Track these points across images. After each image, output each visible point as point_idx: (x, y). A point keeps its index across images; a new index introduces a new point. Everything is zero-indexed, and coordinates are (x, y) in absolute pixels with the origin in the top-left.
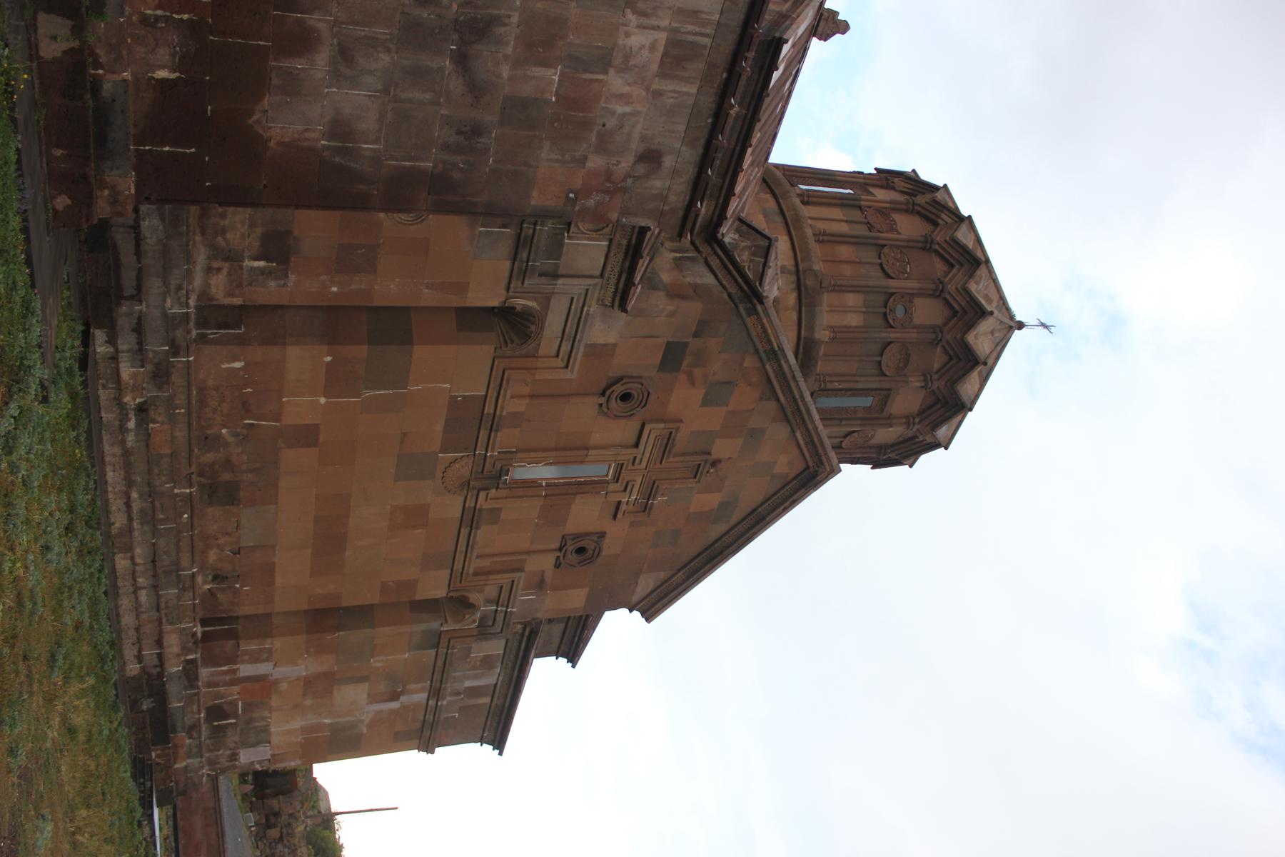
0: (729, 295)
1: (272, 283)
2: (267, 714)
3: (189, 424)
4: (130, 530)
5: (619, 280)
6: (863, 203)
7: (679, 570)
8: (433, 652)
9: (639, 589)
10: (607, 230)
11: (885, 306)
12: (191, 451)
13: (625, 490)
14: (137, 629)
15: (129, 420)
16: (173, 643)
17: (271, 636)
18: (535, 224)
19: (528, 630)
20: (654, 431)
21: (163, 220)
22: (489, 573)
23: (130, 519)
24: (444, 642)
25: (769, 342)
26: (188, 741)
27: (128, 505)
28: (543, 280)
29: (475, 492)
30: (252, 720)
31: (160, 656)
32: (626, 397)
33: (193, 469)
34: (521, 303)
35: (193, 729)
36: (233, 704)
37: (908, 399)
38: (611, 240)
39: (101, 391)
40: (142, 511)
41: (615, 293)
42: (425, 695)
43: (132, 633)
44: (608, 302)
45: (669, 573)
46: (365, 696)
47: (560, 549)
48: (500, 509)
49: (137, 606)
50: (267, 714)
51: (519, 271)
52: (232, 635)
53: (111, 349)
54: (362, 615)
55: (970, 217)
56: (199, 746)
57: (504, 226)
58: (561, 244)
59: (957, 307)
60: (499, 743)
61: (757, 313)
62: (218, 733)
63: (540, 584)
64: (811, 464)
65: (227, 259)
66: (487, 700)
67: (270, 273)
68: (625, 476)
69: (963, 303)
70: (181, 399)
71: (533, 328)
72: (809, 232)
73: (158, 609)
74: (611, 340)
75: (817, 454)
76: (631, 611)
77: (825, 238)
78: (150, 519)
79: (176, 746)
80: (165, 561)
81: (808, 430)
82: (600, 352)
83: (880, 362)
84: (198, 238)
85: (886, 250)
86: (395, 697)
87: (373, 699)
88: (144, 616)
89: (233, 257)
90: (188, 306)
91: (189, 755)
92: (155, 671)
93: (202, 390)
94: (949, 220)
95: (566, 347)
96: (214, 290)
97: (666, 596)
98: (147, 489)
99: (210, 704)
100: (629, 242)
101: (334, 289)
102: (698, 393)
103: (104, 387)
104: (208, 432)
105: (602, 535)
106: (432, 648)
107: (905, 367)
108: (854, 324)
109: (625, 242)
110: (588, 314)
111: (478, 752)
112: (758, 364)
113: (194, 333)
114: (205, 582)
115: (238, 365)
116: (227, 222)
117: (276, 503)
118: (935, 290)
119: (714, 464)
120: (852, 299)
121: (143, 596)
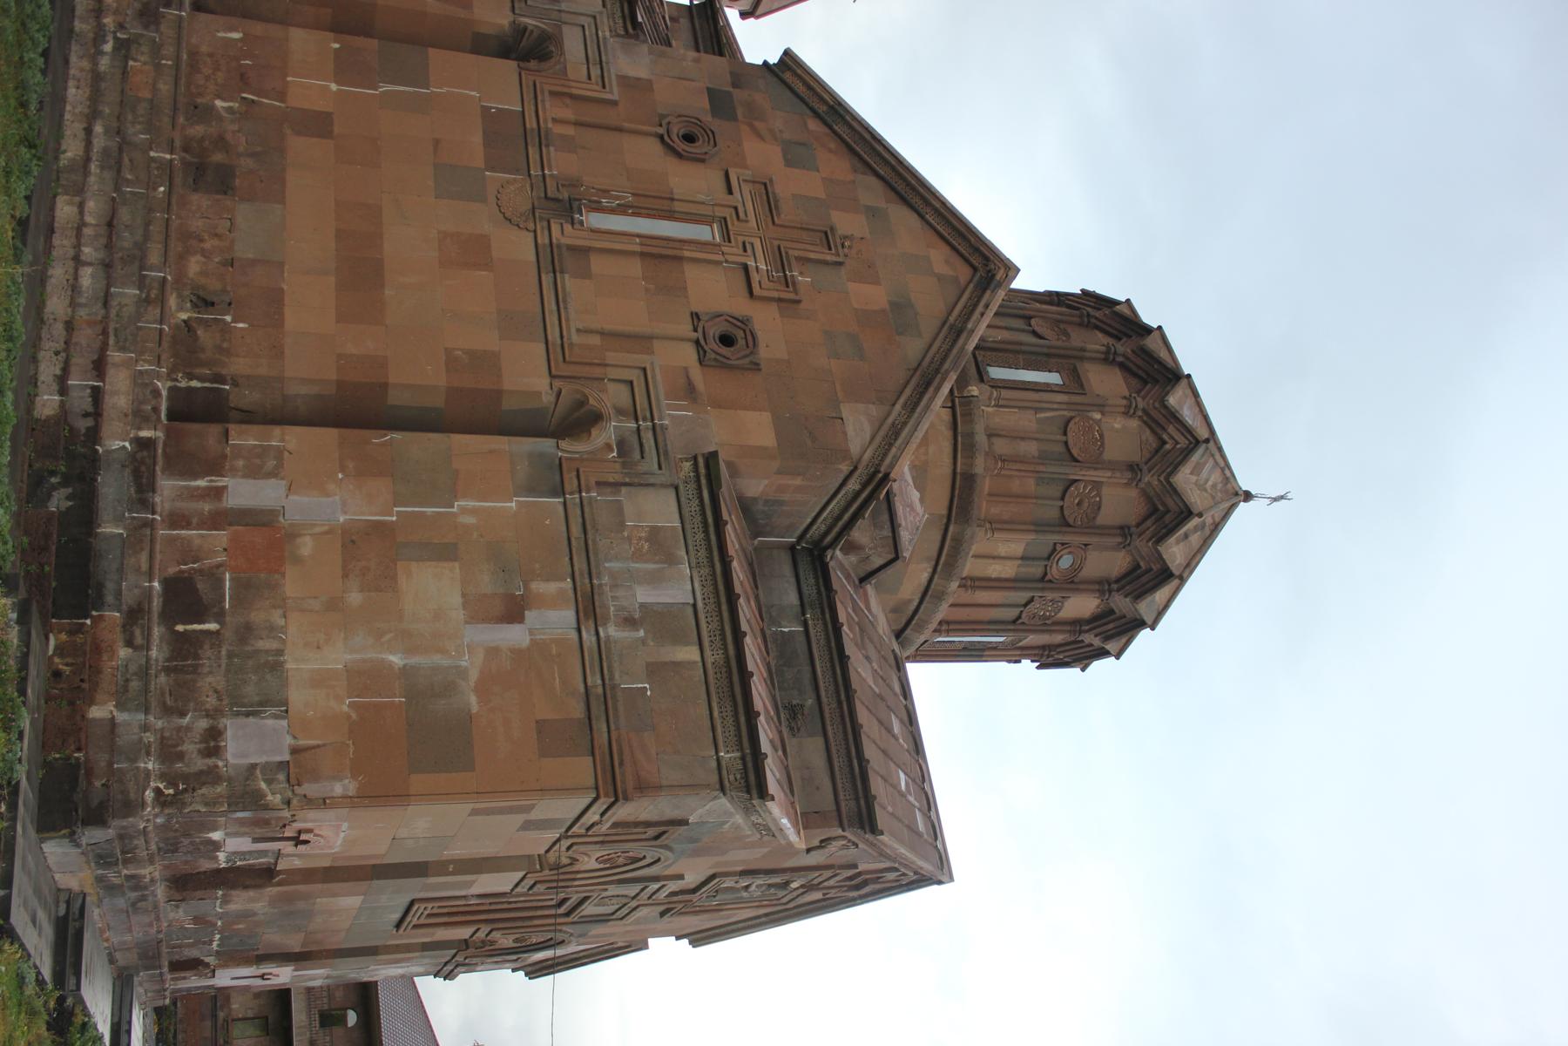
14: (69, 326)
24: (571, 483)
25: (822, 99)
26: (123, 652)
31: (97, 394)
42: (568, 616)
43: (59, 330)
49: (75, 288)
50: (277, 618)
62: (185, 649)
73: (106, 304)
75: (977, 250)
78: (113, 163)
80: (126, 240)
81: (936, 210)
88: (82, 313)
92: (83, 425)
95: (595, 72)
99: (172, 570)
102: (774, 153)
104: (199, 100)
106: (554, 494)
114: (181, 309)
115: (236, 35)
117: (282, 201)
121: (87, 278)
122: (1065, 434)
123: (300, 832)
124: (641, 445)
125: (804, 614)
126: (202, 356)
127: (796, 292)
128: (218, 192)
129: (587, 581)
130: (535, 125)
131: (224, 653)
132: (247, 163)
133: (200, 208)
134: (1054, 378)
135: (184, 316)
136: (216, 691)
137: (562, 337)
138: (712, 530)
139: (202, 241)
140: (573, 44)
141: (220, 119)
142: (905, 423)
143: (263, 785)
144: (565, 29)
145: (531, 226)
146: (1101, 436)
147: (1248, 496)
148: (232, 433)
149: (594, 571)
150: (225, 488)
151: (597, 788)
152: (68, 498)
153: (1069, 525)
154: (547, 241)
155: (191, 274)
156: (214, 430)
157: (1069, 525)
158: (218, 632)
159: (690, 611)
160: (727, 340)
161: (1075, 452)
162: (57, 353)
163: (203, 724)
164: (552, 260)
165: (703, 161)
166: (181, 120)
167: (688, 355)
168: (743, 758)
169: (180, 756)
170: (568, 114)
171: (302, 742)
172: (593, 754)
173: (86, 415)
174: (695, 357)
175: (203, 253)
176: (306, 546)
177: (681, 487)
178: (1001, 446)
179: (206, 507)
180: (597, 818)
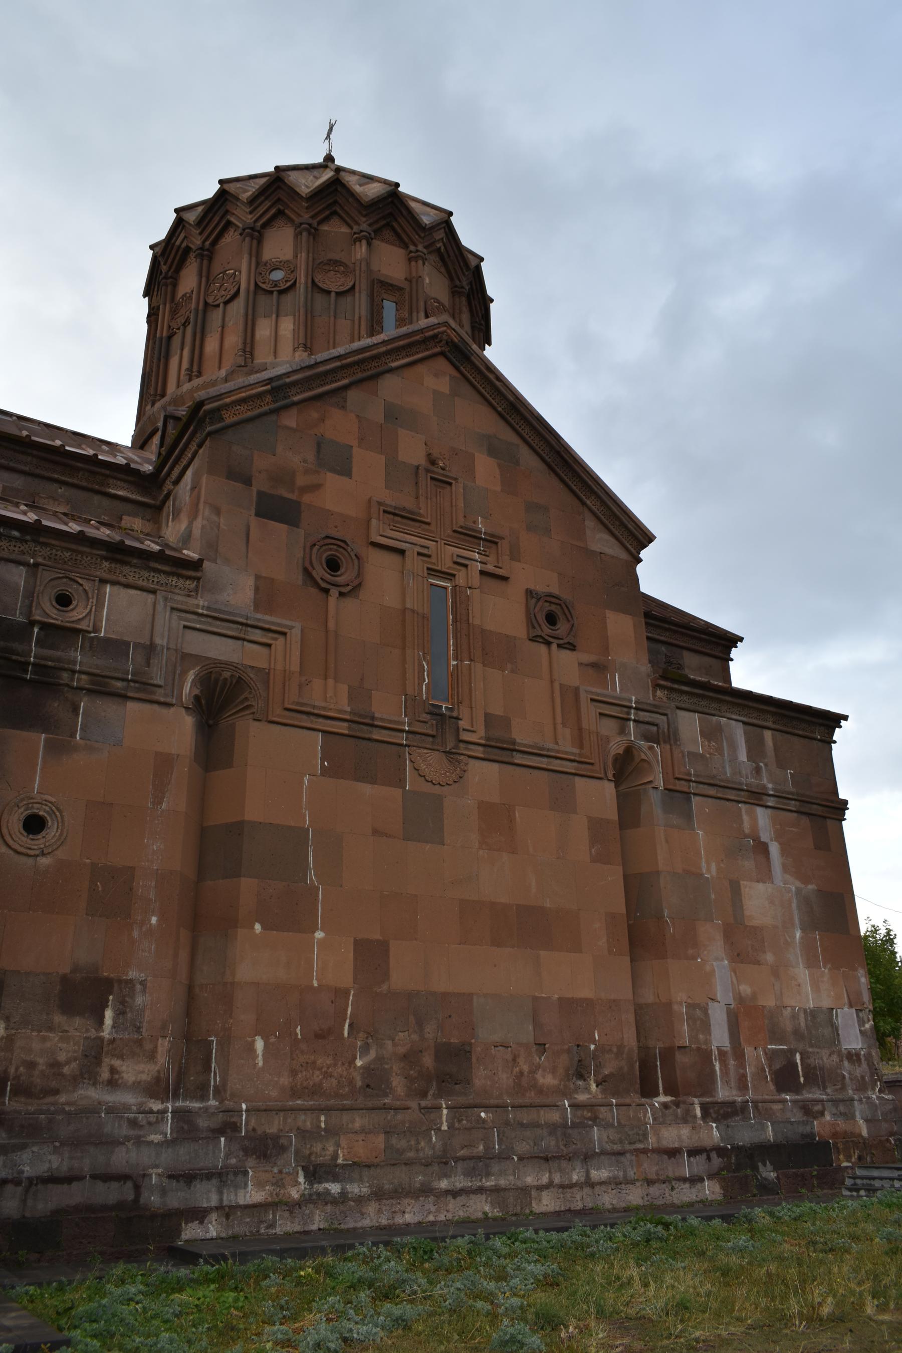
0: (200, 446)
1: (139, 1000)
2: (787, 1012)
3: (344, 1109)
4: (496, 1190)
5: (159, 571)
6: (165, 334)
7: (584, 504)
8: (695, 800)
9: (609, 551)
10: (87, 585)
11: (267, 293)
12: (385, 1108)
13: (466, 566)
14: (650, 1182)
15: (327, 1192)
16: (675, 1135)
17: (669, 1004)
18: (74, 672)
19: (662, 682)
20: (380, 531)
21: (24, 1147)
22: (580, 729)
23: (481, 1190)
24: (682, 786)
25: (260, 396)
26: (828, 1117)
27: (455, 1193)
28: (154, 661)
29: (462, 745)
30: (796, 1032)
31: (694, 1152)
32: (333, 565)
33: (413, 1104)
34: (188, 688)
35: (808, 1110)
36: (771, 1056)
37: (390, 261)
38: (103, 581)
39: (278, 1230)
40: (469, 1174)
41: (179, 576)
42: (760, 811)
43: (654, 1190)
44: (191, 585)
45: (587, 514)
46: (761, 886)
47: (548, 644)
48: (487, 715)
49: (615, 1183)
50: (787, 1012)
51: (143, 689)
52: (668, 1054)
53: (214, 1216)
54: (638, 889)
55: (177, 211)
56: (835, 1102)
57: (75, 710)
58: (107, 641)
59: (273, 211)
60: (831, 721)
61: (218, 409)
62: (815, 1077)
63: (599, 668)
64: (438, 350)
65: (98, 1061)
66: (768, 734)
67: (123, 1002)
68: (446, 565)
69: (268, 204)
70: (305, 1121)
71: (226, 674)
72: (187, 387)
74: (251, 582)
75: (425, 341)
76: (640, 560)
77: (195, 368)
78: (479, 1164)
79: (835, 1135)
80: (549, 1143)
81: (388, 353)
82: (267, 594)
83: (338, 294)
84: (62, 1098)
85: (210, 300)
86: (762, 849)
87: (765, 875)
88: (631, 1174)
89: (95, 1053)
90: (165, 1111)
91: (849, 1116)
92: (717, 1161)
93: (295, 1092)
94: (182, 235)
95: (257, 635)
96: (144, 1077)
97: (618, 518)
98: (436, 1168)
99: (772, 1087)
100: (106, 559)
101: (154, 920)
102: (332, 480)
103: (272, 1226)
104: (359, 1083)
105: (529, 593)
106: (689, 800)
107: (346, 266)
108: (291, 327)
109: (106, 564)
110: (208, 608)
111: (845, 748)
112: (294, 411)
113: (213, 1103)
114: (587, 1089)
115: (259, 1044)
116: (41, 1061)
117: (471, 995)
118: (252, 238)
119: (433, 462)
120: (264, 330)
124: (648, 723)
126: (626, 1069)
127: (502, 538)
128: (469, 1059)
129: (742, 793)
130: (346, 724)
131: (811, 1050)
132: (430, 1031)
133: (489, 1077)
135: (593, 1086)
136: (830, 1055)
137: (574, 761)
139: (521, 1073)
141: (380, 1059)
148: (681, 1043)
150: (718, 1048)
152: (765, 1165)
154: (481, 748)
155: (556, 1082)
156: (681, 1059)
158: (801, 1054)
162: (673, 1189)
163: (846, 1063)
169: (863, 1077)
173: (709, 1158)
174: (568, 652)
175: (533, 1072)
176: (745, 989)
179: (732, 1062)
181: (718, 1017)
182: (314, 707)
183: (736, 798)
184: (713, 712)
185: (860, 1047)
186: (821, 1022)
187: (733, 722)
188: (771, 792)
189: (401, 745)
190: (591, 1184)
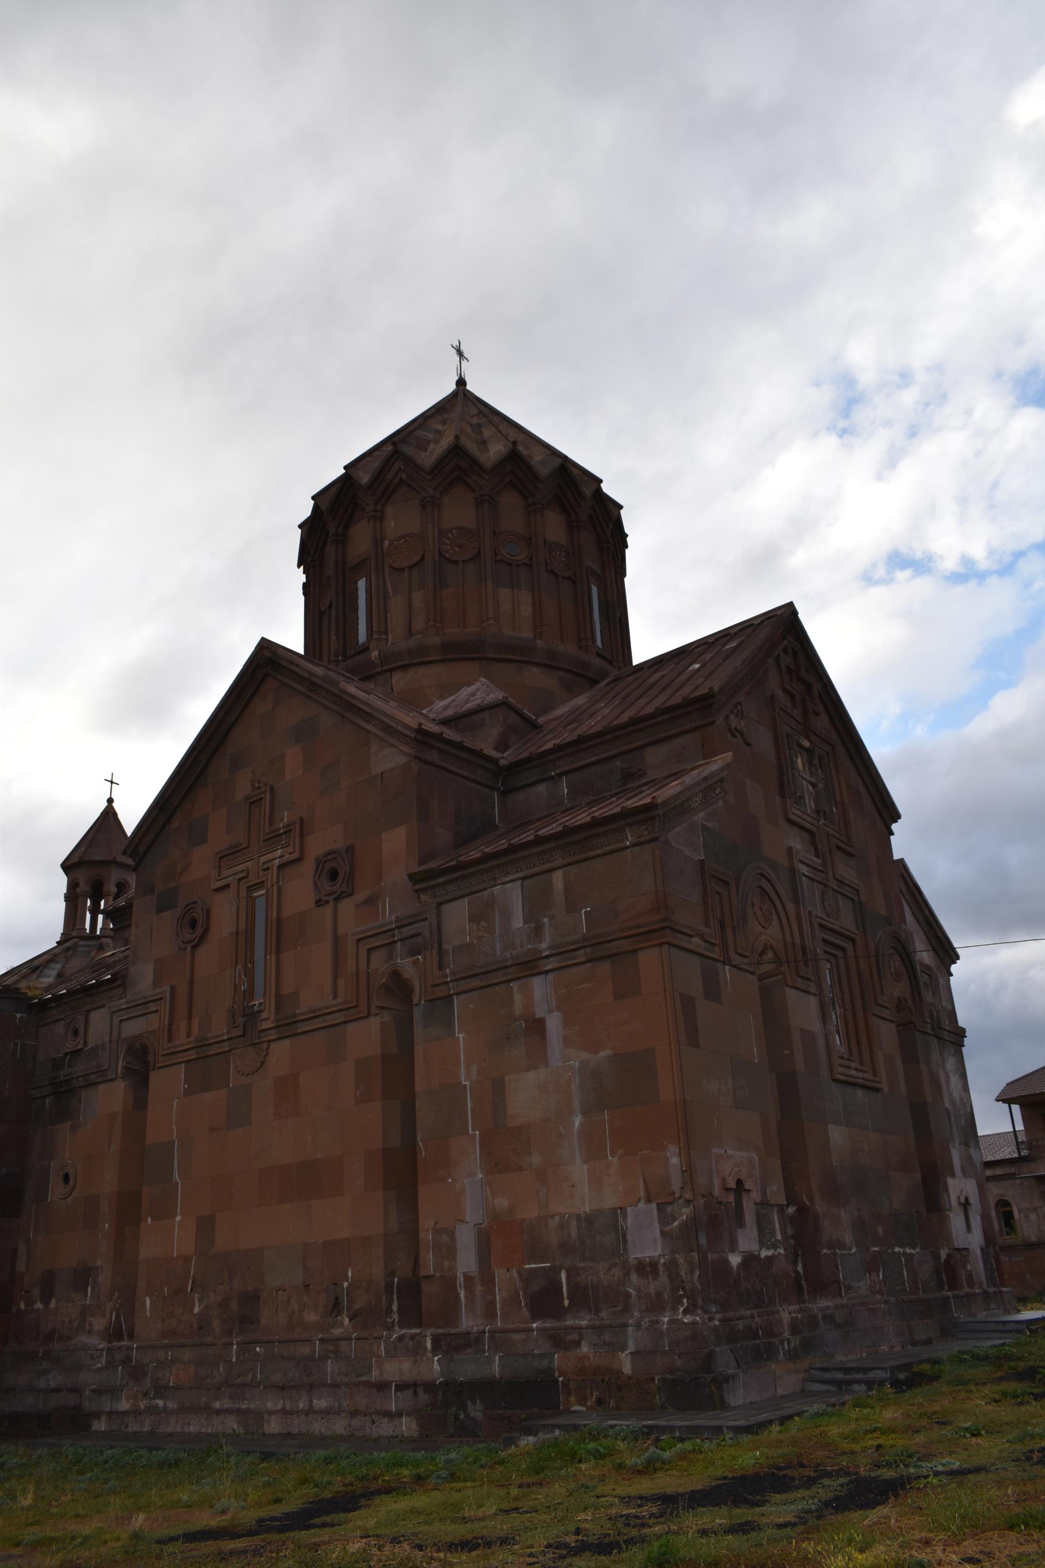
14: (354, 1413)
26: (585, 1348)
29: (262, 1034)
31: (401, 1387)
39: (129, 1430)
41: (115, 988)
42: (537, 982)
43: (356, 1422)
49: (326, 1413)
50: (554, 1223)
53: (104, 1418)
84: (73, 1342)
92: (423, 1397)
95: (152, 1007)
99: (526, 1313)
103: (127, 1426)
110: (127, 1003)
115: (148, 1302)
121: (320, 1403)
122: (403, 569)
123: (728, 1190)
125: (552, 778)
127: (294, 823)
129: (510, 970)
130: (193, 1051)
131: (582, 1265)
134: (362, 584)
135: (347, 1321)
136: (610, 1269)
137: (340, 1011)
138: (466, 872)
140: (133, 1028)
142: (381, 721)
143: (676, 1224)
144: (124, 1035)
145: (265, 1045)
146: (401, 537)
147: (461, 382)
149: (502, 965)
150: (464, 1274)
151: (661, 945)
152: (474, 1403)
153: (479, 553)
154: (274, 1031)
156: (427, 1288)
157: (479, 553)
158: (568, 1271)
159: (527, 882)
160: (333, 875)
161: (417, 558)
162: (374, 1422)
163: (634, 1277)
164: (288, 1026)
165: (208, 911)
166: (210, 1339)
167: (347, 906)
168: (630, 825)
169: (659, 1294)
170: (184, 1024)
171: (642, 1193)
172: (636, 951)
173: (415, 1394)
174: (347, 900)
176: (502, 1203)
177: (439, 900)
178: (419, 623)
179: (479, 1288)
180: (696, 940)
181: (466, 1239)
182: (176, 1047)
183: (506, 978)
184: (481, 887)
185: (657, 1254)
186: (605, 1229)
187: (510, 885)
188: (547, 953)
189: (226, 1052)
190: (309, 1411)
